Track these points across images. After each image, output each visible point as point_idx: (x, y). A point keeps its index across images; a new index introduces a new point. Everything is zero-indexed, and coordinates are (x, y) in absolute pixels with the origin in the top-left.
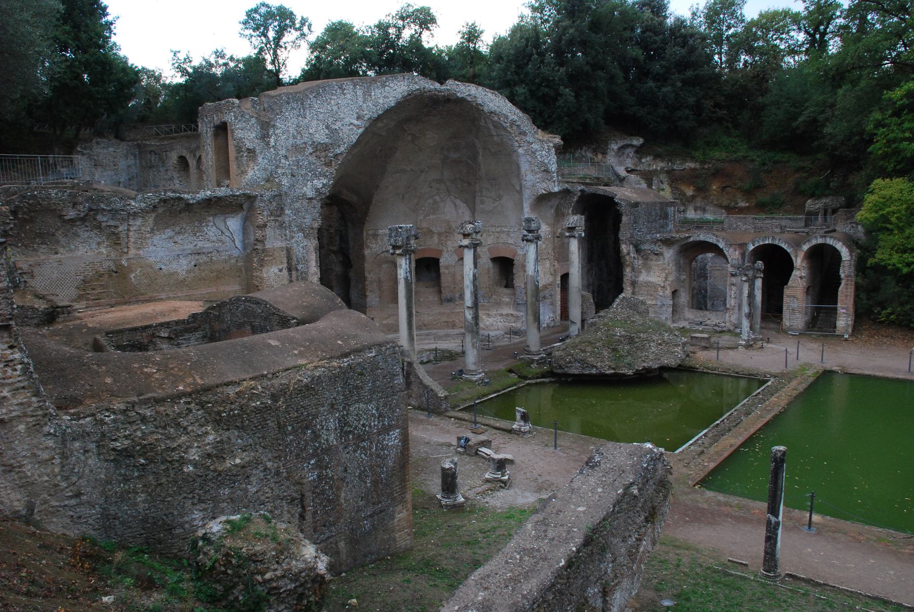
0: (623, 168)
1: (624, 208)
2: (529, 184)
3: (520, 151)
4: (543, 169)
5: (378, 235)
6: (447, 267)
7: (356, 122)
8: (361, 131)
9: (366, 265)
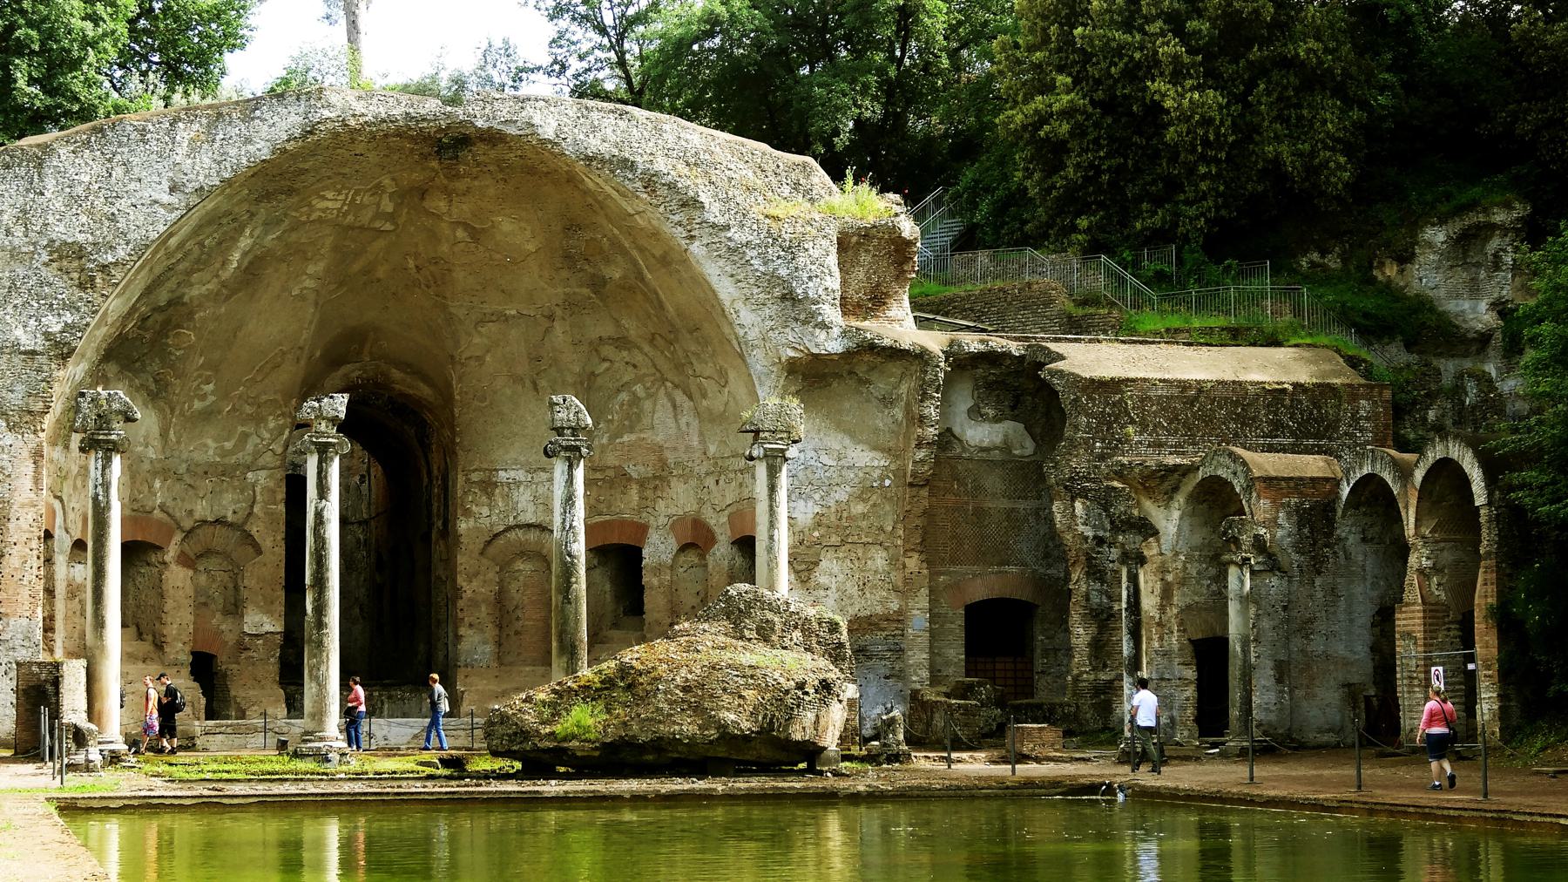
0: (1483, 306)
1: (1066, 398)
2: (753, 334)
3: (696, 248)
4: (777, 292)
5: (495, 485)
6: (658, 570)
7: (166, 198)
8: (178, 213)
9: (460, 559)
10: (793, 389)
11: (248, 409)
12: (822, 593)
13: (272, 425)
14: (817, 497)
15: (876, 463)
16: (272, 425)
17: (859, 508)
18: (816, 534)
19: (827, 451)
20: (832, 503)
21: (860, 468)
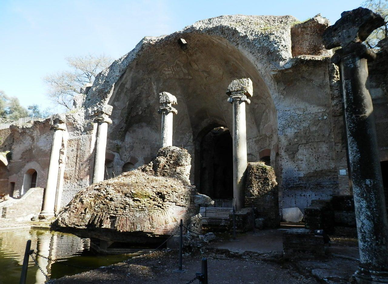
4: (266, 52)
10: (282, 88)
11: (181, 132)
12: (300, 162)
13: (188, 135)
14: (296, 126)
15: (320, 111)
16: (188, 135)
17: (314, 129)
18: (296, 140)
19: (299, 109)
20: (302, 128)
21: (313, 114)
